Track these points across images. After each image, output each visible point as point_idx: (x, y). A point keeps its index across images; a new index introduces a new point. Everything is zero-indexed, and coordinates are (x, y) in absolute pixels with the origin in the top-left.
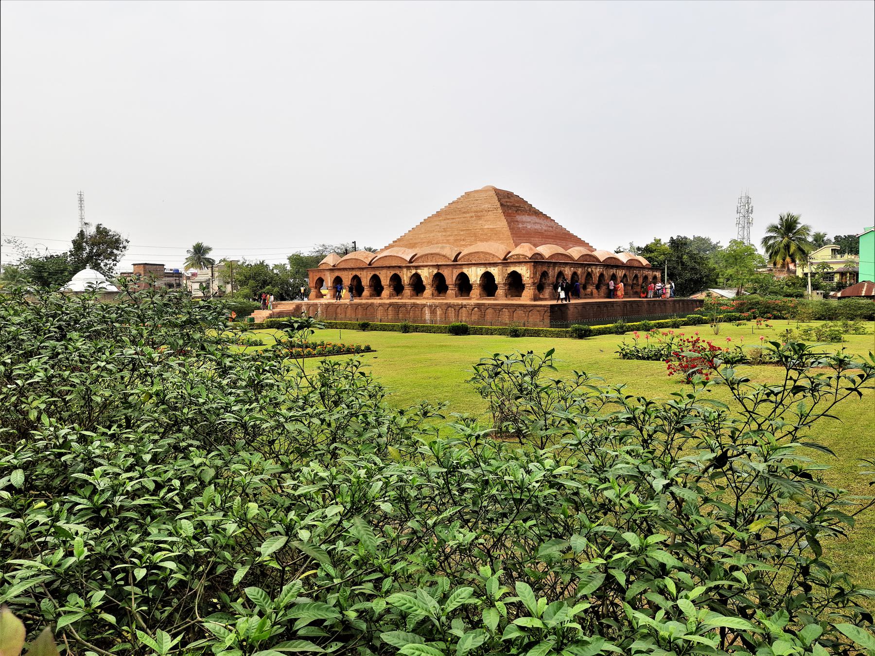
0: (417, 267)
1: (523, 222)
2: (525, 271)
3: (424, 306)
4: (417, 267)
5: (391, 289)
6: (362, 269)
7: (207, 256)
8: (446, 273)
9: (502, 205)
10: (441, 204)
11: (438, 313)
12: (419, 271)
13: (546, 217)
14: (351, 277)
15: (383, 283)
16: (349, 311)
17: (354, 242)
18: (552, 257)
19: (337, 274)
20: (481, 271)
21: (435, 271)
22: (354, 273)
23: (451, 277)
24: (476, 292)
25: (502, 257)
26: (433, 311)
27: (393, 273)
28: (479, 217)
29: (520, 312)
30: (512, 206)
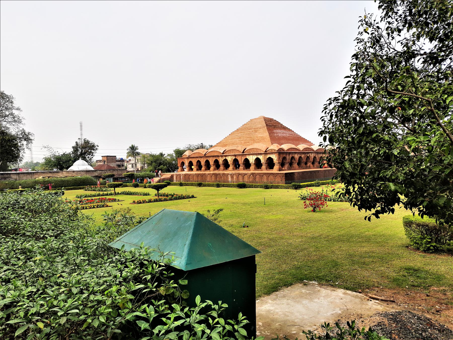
0: (226, 156)
1: (277, 133)
2: (275, 157)
3: (228, 174)
4: (226, 156)
5: (215, 166)
6: (201, 157)
7: (137, 151)
8: (239, 158)
9: (267, 125)
10: (239, 126)
11: (235, 177)
12: (227, 158)
13: (289, 130)
14: (196, 161)
15: (211, 164)
16: (195, 178)
17: (202, 144)
18: (288, 150)
19: (190, 160)
20: (255, 157)
21: (234, 158)
22: (198, 159)
23: (241, 160)
24: (252, 167)
25: (264, 151)
26: (232, 177)
27: (215, 159)
28: (256, 131)
29: (271, 177)
30: (272, 125)
